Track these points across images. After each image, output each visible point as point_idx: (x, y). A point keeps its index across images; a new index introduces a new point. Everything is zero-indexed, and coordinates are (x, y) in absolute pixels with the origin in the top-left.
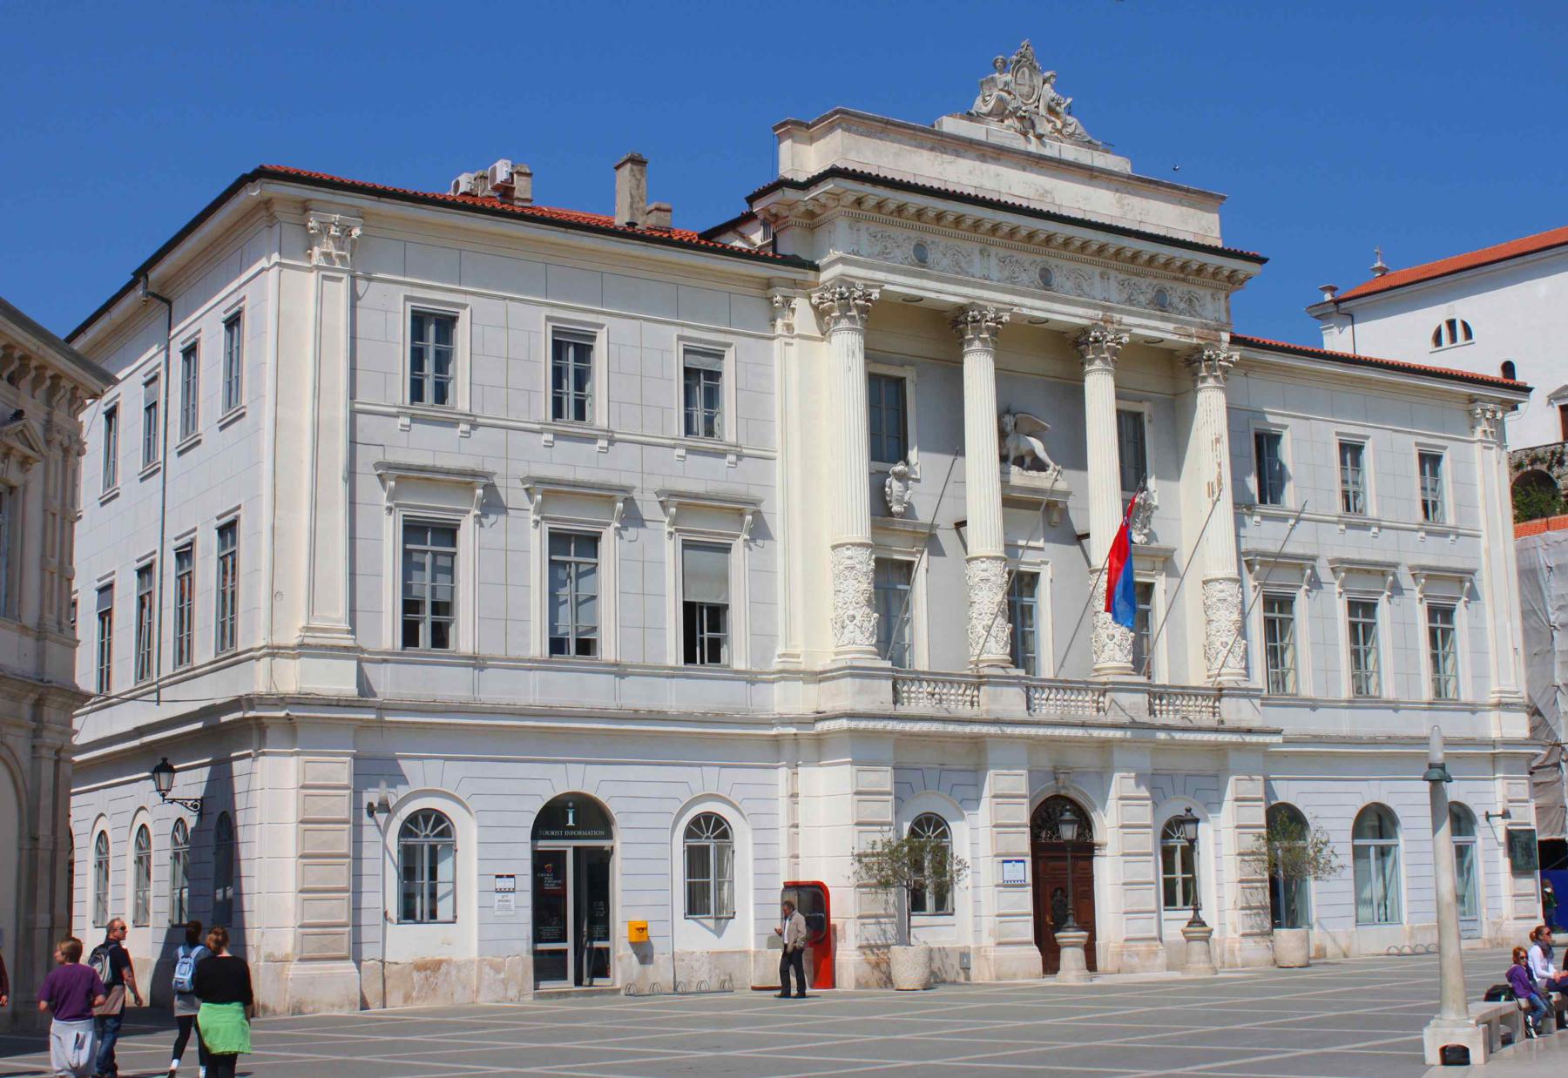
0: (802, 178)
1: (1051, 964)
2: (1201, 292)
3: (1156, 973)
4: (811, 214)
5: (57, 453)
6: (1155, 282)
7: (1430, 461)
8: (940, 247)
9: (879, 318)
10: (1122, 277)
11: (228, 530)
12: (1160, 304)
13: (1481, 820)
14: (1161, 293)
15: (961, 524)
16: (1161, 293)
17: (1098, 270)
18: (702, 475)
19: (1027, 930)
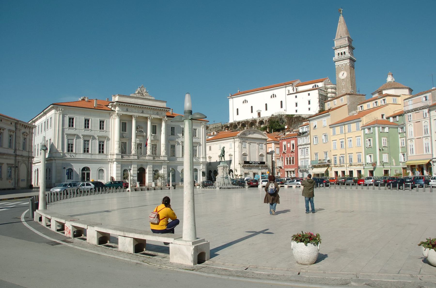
8: (129, 109)
12: (157, 114)
14: (158, 112)
16: (158, 112)
18: (102, 134)
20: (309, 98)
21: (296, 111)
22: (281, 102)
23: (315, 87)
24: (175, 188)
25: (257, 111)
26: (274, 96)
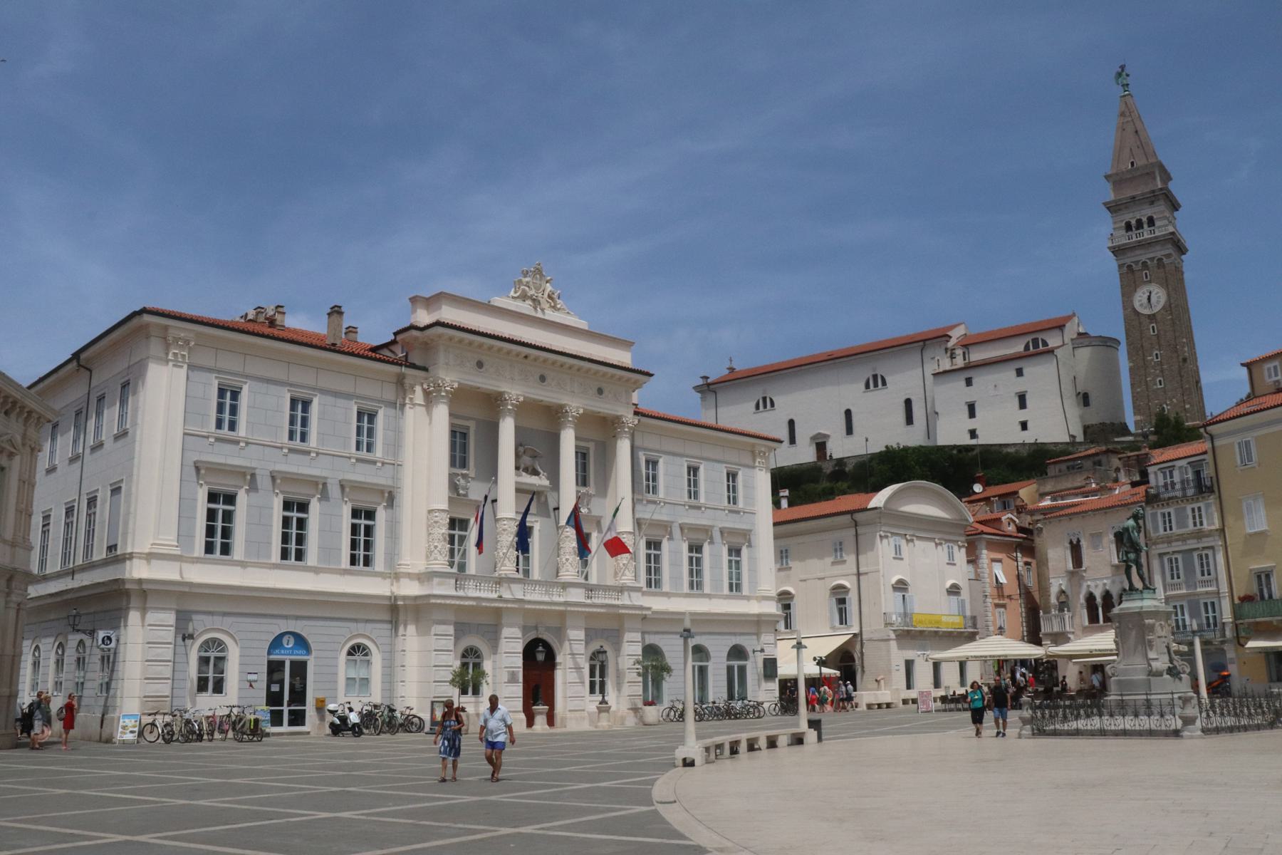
0: (422, 325)
1: (530, 723)
3: (586, 726)
4: (426, 344)
5: (28, 449)
7: (732, 476)
9: (459, 397)
11: (116, 490)
13: (751, 654)
15: (494, 501)
19: (519, 704)
20: (1021, 385)
21: (973, 434)
22: (908, 403)
23: (1036, 345)
24: (820, 739)
25: (813, 438)
26: (877, 381)
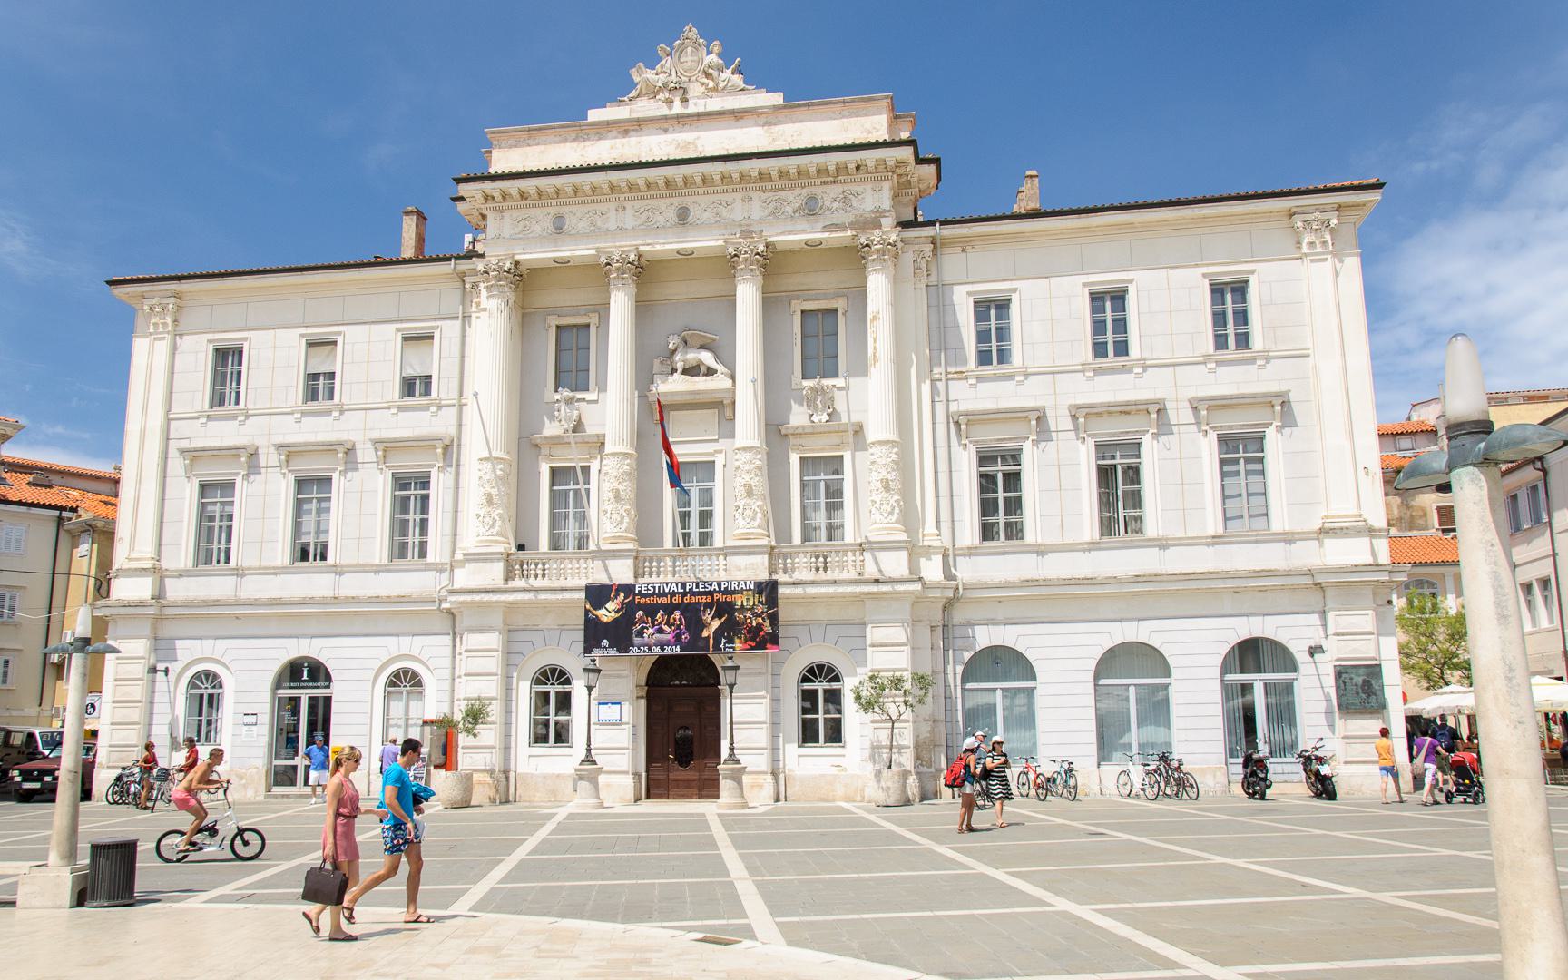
2: (859, 189)
6: (805, 192)
10: (764, 196)
12: (811, 209)
16: (812, 198)
17: (739, 196)
